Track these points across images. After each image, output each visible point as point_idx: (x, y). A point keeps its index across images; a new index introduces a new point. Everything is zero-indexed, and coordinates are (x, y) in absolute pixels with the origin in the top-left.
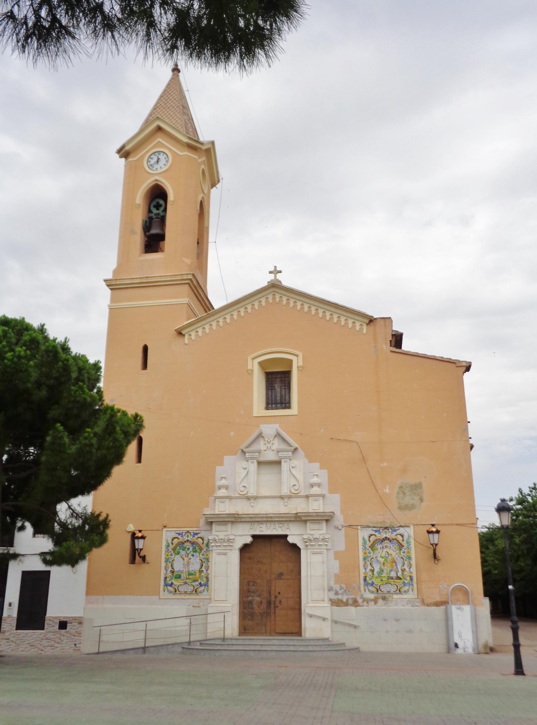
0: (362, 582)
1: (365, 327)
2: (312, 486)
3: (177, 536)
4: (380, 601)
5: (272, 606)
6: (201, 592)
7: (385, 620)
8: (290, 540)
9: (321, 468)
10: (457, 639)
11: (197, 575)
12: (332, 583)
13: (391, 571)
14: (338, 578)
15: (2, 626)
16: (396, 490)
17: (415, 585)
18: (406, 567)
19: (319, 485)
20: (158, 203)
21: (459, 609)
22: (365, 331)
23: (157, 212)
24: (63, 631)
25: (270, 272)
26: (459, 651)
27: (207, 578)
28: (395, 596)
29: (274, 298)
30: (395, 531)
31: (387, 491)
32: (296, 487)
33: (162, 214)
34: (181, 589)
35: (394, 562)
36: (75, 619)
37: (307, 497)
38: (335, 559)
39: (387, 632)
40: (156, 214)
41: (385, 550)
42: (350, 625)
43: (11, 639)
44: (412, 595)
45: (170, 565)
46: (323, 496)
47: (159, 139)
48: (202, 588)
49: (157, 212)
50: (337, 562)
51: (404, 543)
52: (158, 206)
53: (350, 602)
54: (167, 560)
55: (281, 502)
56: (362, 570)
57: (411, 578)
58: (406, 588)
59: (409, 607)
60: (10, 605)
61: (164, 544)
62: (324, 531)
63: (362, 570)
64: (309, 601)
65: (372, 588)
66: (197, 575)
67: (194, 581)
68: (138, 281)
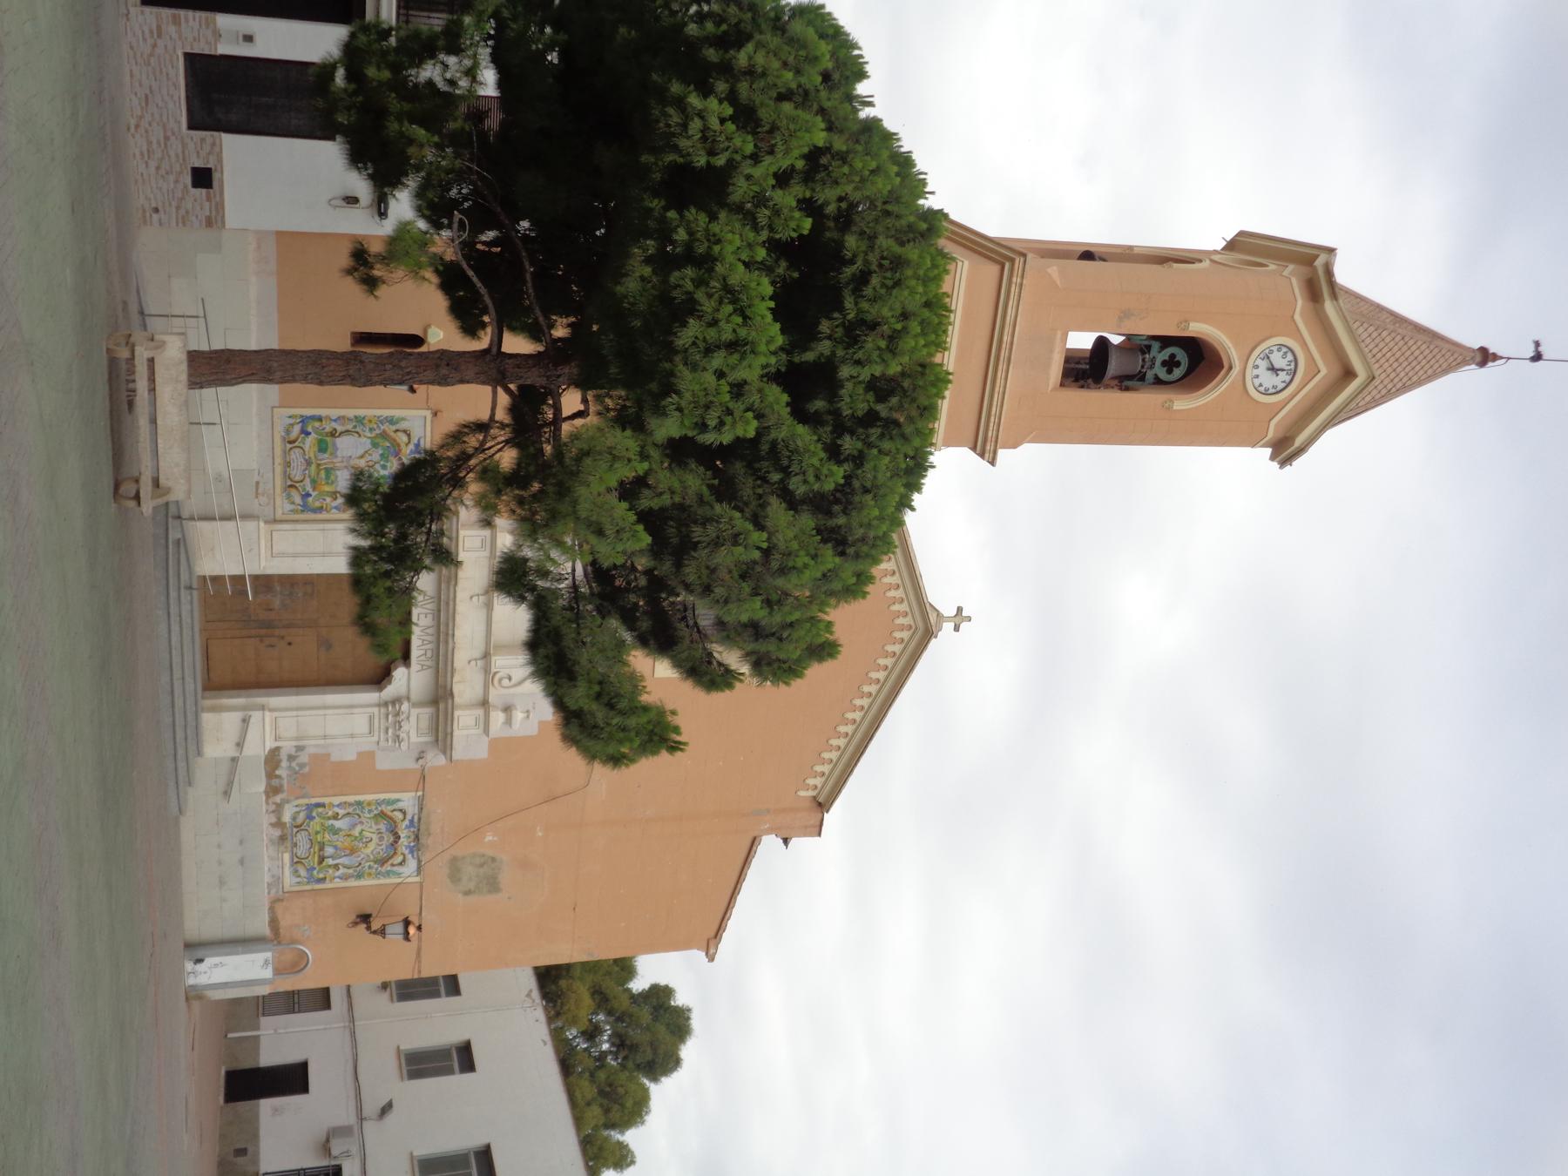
0: (314, 801)
1: (814, 793)
2: (507, 709)
3: (415, 440)
4: (277, 833)
5: (263, 632)
6: (289, 497)
7: (241, 842)
8: (399, 673)
9: (541, 723)
10: (209, 961)
11: (327, 488)
12: (312, 750)
13: (336, 847)
14: (321, 759)
15: (190, 13)
16: (490, 853)
17: (308, 887)
18: (342, 871)
19: (509, 721)
20: (1178, 364)
21: (266, 962)
22: (802, 793)
23: (1158, 363)
24: (188, 179)
25: (960, 610)
26: (189, 966)
27: (320, 509)
28: (287, 857)
29: (902, 628)
30: (412, 852)
31: (489, 838)
32: (506, 682)
33: (1150, 375)
34: (296, 456)
35: (353, 851)
36: (220, 207)
37: (484, 703)
38: (359, 754)
39: (219, 846)
40: (1153, 360)
41: (374, 837)
42: (230, 784)
43: (160, 43)
44: (289, 880)
45: (350, 427)
46: (486, 731)
47: (1324, 371)
48: (298, 500)
49: (1158, 363)
50: (350, 756)
51: (387, 867)
52: (1171, 364)
53: (275, 782)
54: (359, 420)
55: (478, 653)
56: (336, 800)
57: (323, 880)
58: (303, 872)
59: (267, 878)
60: (249, 38)
61: (397, 413)
62: (414, 738)
63: (336, 800)
64: (276, 714)
65: (302, 816)
66: (327, 488)
67: (314, 482)
68: (1006, 338)
